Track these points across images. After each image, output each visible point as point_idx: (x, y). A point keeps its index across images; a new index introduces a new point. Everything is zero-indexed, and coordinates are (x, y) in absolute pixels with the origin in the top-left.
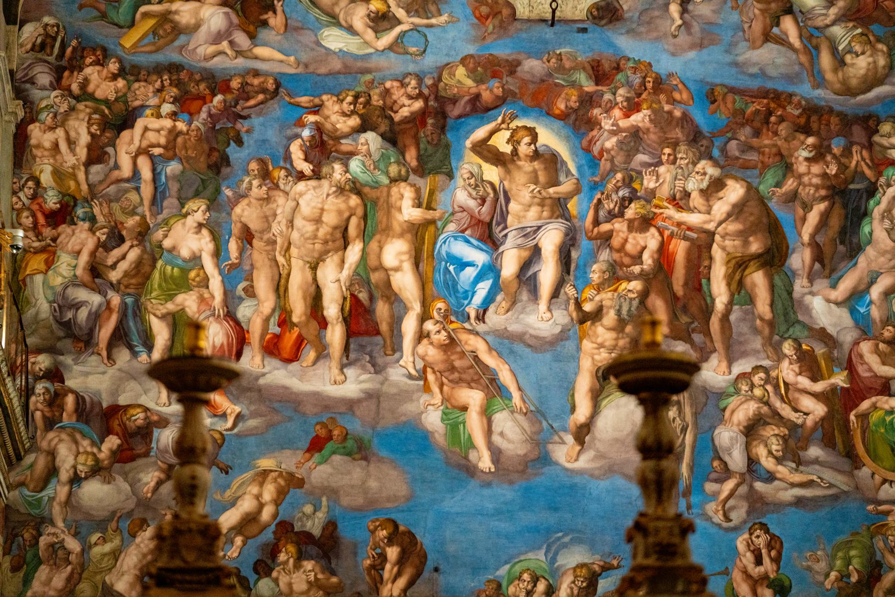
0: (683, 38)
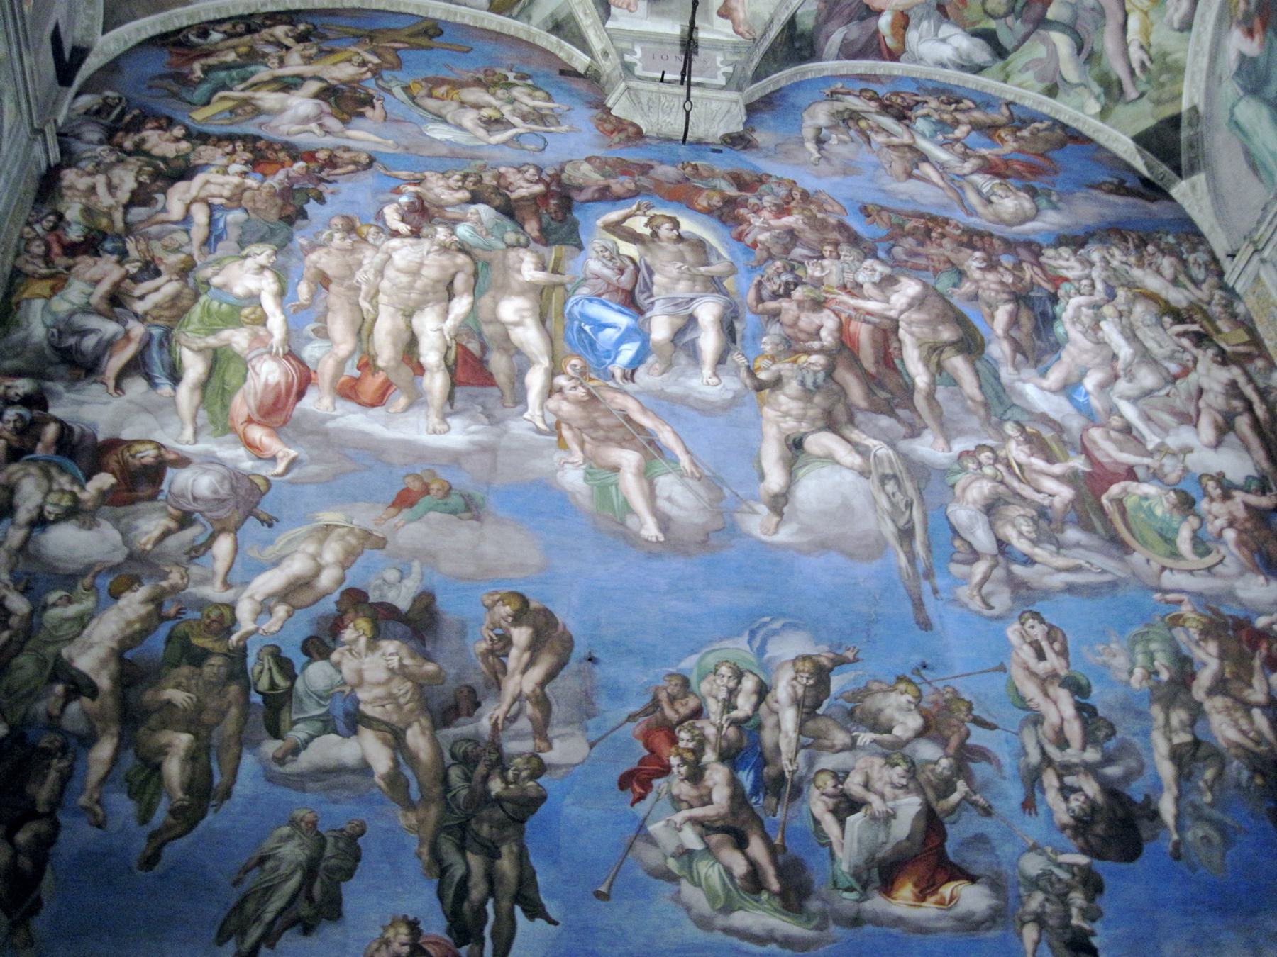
0: (823, 166)
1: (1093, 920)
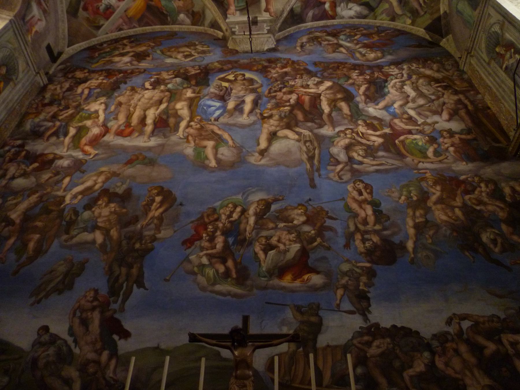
0: (302, 53)
1: (370, 287)
